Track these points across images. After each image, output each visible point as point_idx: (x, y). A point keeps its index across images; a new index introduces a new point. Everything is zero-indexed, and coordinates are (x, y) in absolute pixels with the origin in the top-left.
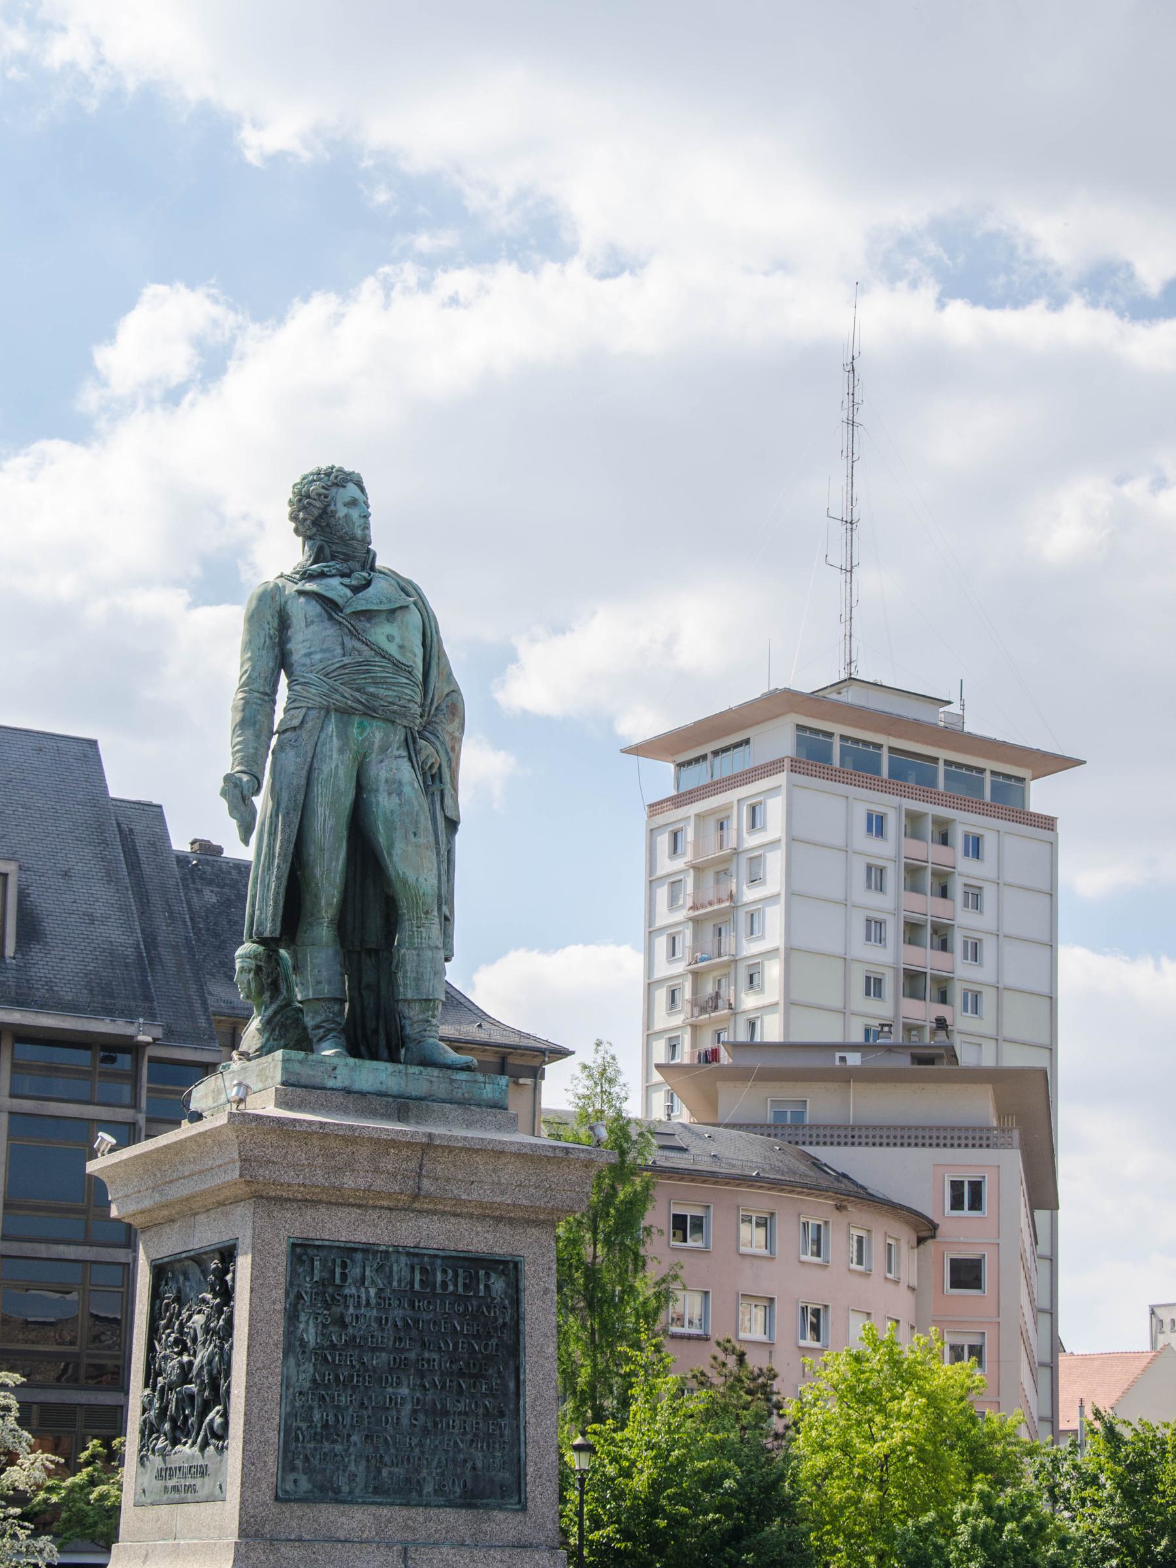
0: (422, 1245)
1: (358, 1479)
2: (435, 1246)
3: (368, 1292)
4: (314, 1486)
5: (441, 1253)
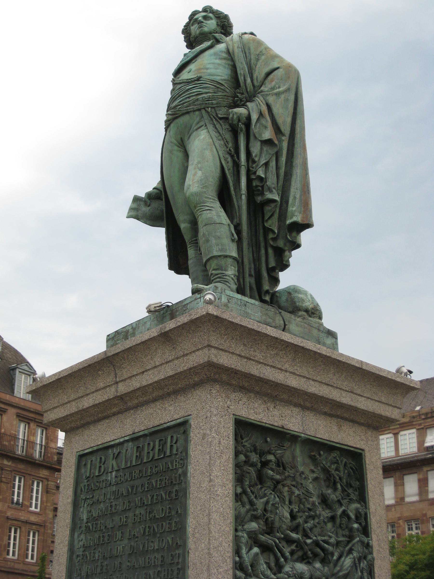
0: (136, 431)
2: (143, 429)
3: (111, 475)
5: (146, 432)
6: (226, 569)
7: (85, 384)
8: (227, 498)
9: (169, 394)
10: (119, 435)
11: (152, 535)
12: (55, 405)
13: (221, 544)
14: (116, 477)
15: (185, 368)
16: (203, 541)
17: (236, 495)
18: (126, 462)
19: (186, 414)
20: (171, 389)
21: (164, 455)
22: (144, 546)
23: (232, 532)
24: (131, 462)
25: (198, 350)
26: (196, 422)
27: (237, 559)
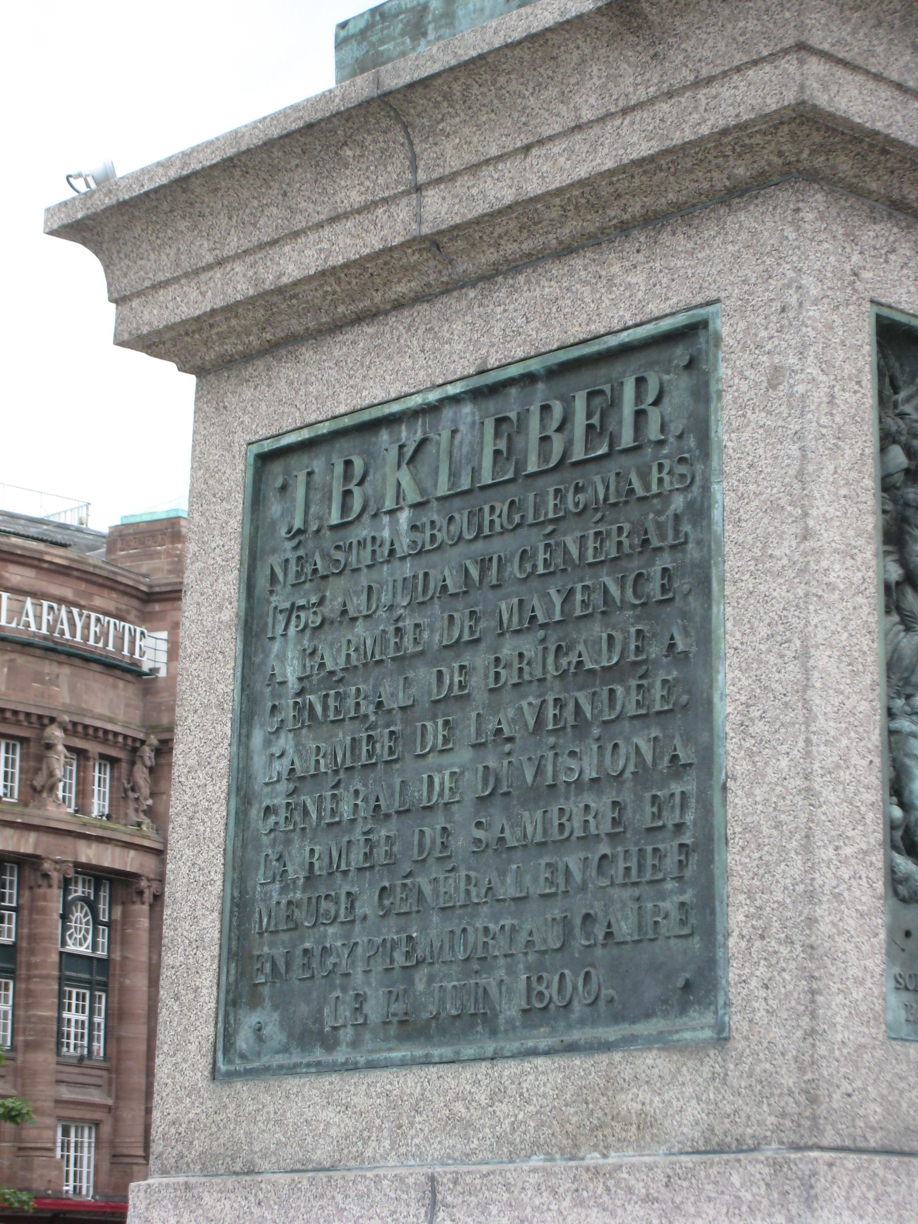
0: (492, 362)
1: (367, 1008)
2: (520, 354)
3: (394, 523)
4: (290, 1036)
5: (534, 366)
6: (864, 846)
7: (285, 194)
8: (860, 599)
9: (624, 229)
10: (422, 378)
11: (569, 729)
12: (161, 277)
13: (844, 758)
14: (414, 528)
15: (705, 130)
16: (784, 748)
17: (888, 588)
18: (454, 475)
19: (699, 299)
20: (636, 208)
21: (611, 446)
22: (539, 771)
23: (879, 717)
24: (475, 472)
25: (755, 63)
26: (742, 325)
27: (897, 813)
